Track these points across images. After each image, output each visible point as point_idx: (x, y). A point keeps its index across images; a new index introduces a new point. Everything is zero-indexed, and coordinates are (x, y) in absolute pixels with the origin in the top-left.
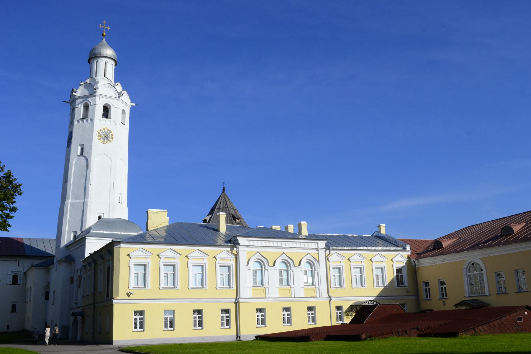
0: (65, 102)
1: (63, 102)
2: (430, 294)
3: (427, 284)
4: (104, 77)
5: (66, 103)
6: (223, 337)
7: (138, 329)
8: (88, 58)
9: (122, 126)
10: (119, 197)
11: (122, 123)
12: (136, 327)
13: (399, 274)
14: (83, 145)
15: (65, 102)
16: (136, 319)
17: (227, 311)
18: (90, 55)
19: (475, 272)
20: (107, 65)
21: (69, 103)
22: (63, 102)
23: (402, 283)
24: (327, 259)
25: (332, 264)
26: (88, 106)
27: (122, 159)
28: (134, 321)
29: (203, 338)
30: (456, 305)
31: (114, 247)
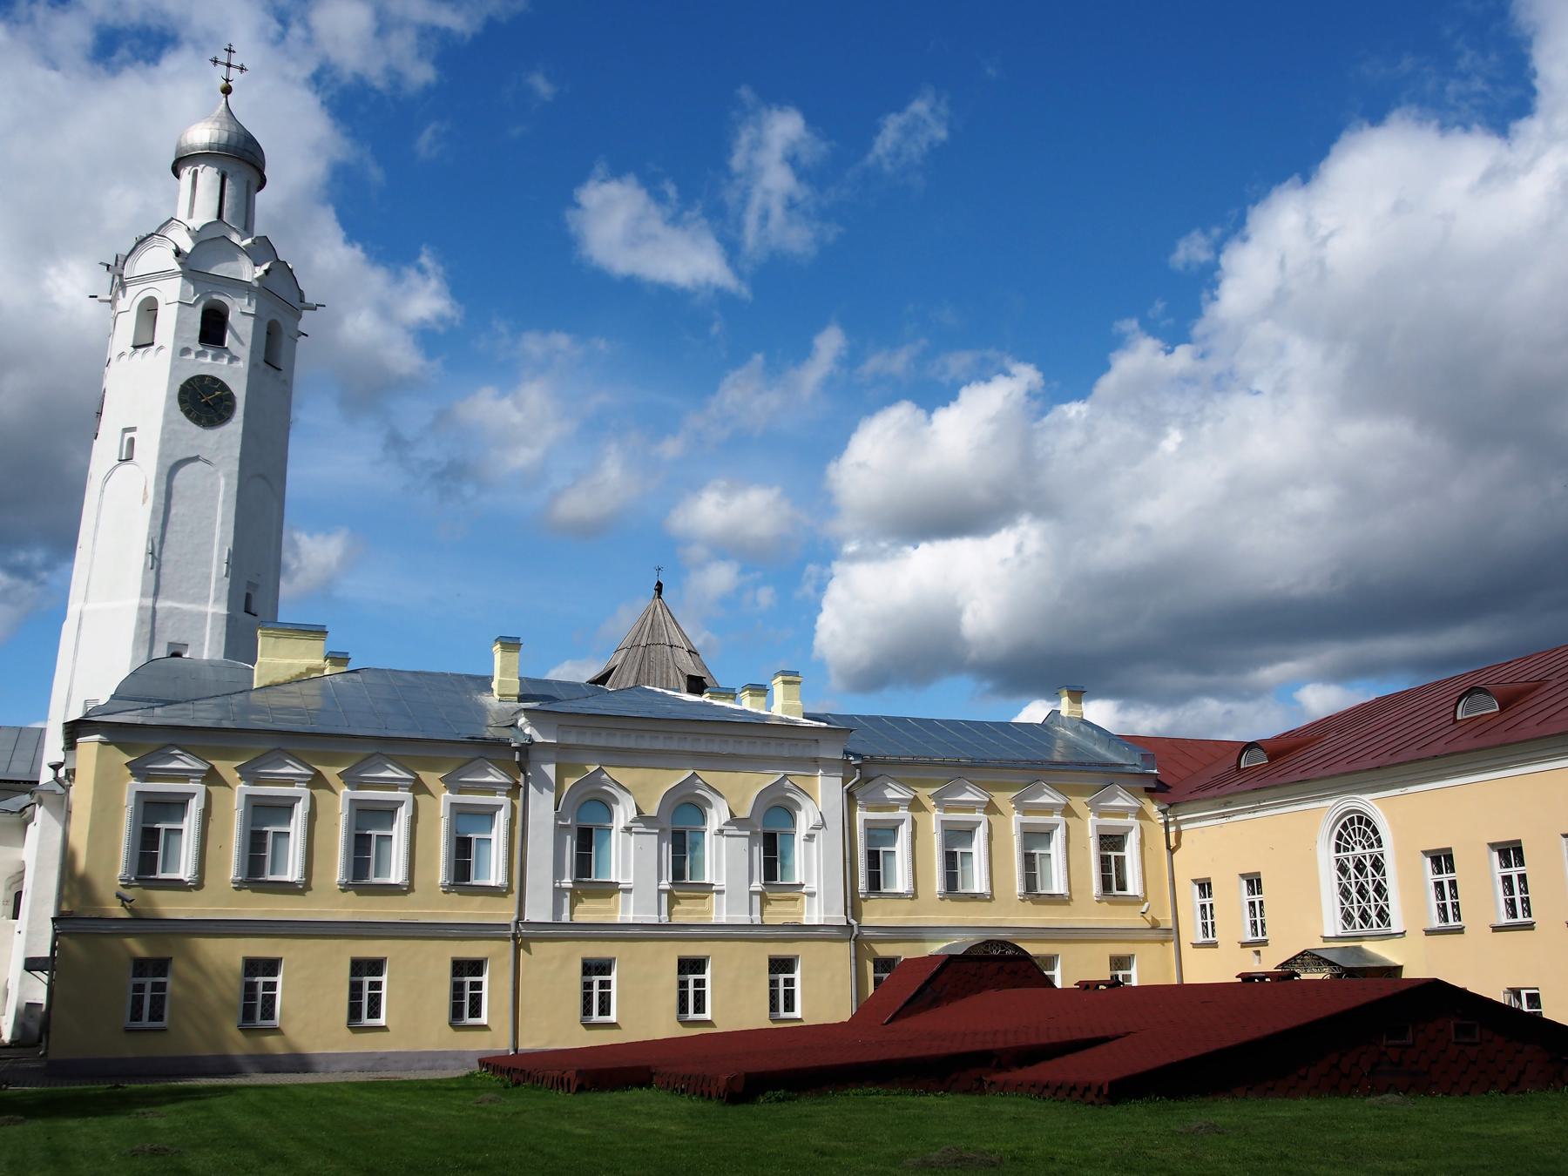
1: (91, 297)
2: (1213, 923)
3: (1205, 887)
6: (458, 1056)
7: (145, 1023)
8: (174, 159)
10: (248, 597)
11: (266, 362)
12: (136, 1015)
13: (1113, 854)
14: (133, 429)
15: (96, 297)
16: (139, 988)
17: (476, 967)
18: (177, 153)
19: (1359, 849)
20: (228, 182)
22: (91, 297)
23: (1122, 886)
24: (850, 796)
25: (861, 816)
27: (263, 477)
28: (130, 993)
29: (382, 1060)
30: (1276, 968)
31: (78, 740)
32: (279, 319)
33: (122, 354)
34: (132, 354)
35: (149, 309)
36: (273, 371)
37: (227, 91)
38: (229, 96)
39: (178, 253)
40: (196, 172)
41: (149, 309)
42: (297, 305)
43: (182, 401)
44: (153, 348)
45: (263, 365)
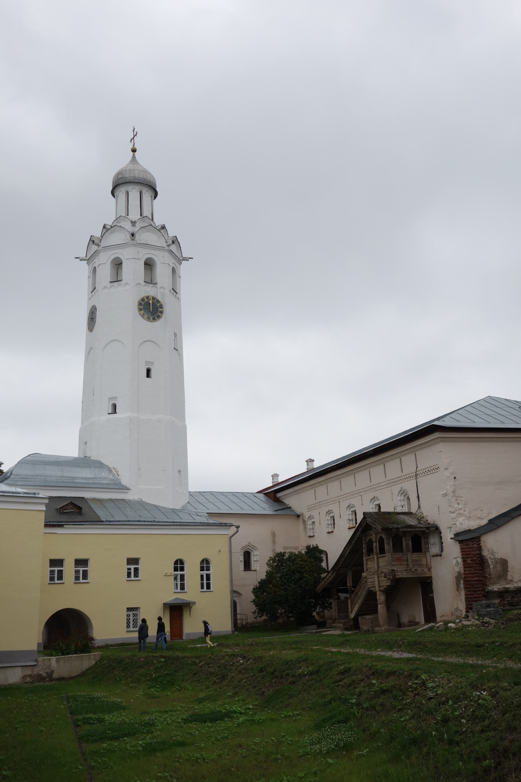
0: (78, 258)
1: (76, 258)
4: (141, 216)
5: (81, 260)
9: (173, 293)
11: (173, 289)
15: (78, 258)
18: (113, 184)
21: (85, 260)
22: (76, 258)
26: (121, 263)
32: (175, 267)
33: (105, 287)
34: (111, 287)
35: (118, 264)
36: (175, 294)
37: (134, 151)
38: (135, 153)
39: (133, 235)
40: (128, 193)
41: (118, 264)
42: (181, 258)
43: (140, 310)
44: (122, 283)
45: (172, 291)
